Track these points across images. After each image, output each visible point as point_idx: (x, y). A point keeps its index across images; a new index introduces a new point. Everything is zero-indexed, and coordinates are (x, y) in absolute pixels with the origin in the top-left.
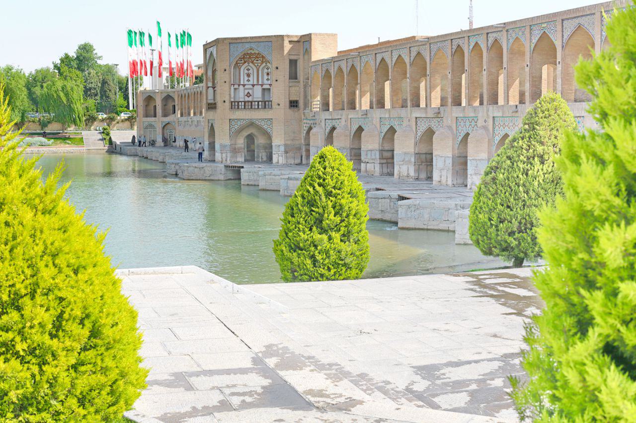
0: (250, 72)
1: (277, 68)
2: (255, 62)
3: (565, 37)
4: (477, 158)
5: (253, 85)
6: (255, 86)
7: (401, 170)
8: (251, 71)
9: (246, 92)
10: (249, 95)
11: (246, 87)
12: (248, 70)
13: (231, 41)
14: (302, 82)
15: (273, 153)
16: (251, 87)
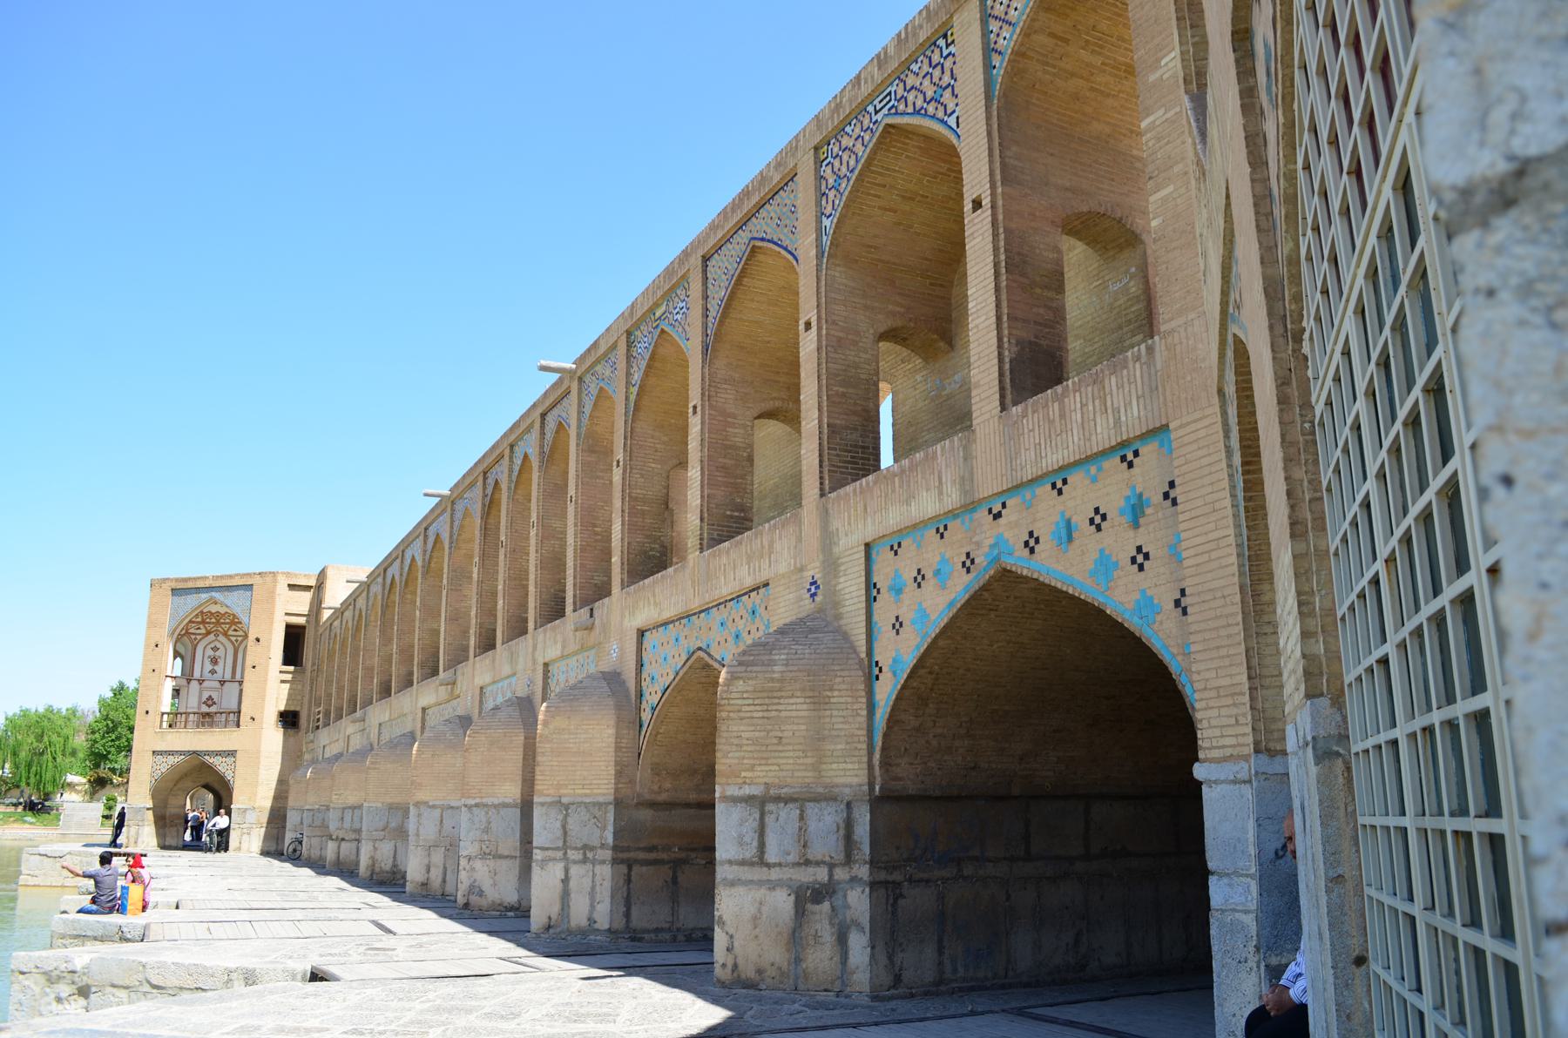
0: (217, 653)
1: (258, 640)
2: (231, 633)
3: (712, 313)
4: (489, 801)
5: (222, 683)
6: (227, 684)
7: (378, 856)
8: (220, 653)
9: (205, 695)
10: (210, 702)
11: (206, 684)
12: (215, 649)
13: (174, 585)
14: (308, 673)
16: (217, 685)
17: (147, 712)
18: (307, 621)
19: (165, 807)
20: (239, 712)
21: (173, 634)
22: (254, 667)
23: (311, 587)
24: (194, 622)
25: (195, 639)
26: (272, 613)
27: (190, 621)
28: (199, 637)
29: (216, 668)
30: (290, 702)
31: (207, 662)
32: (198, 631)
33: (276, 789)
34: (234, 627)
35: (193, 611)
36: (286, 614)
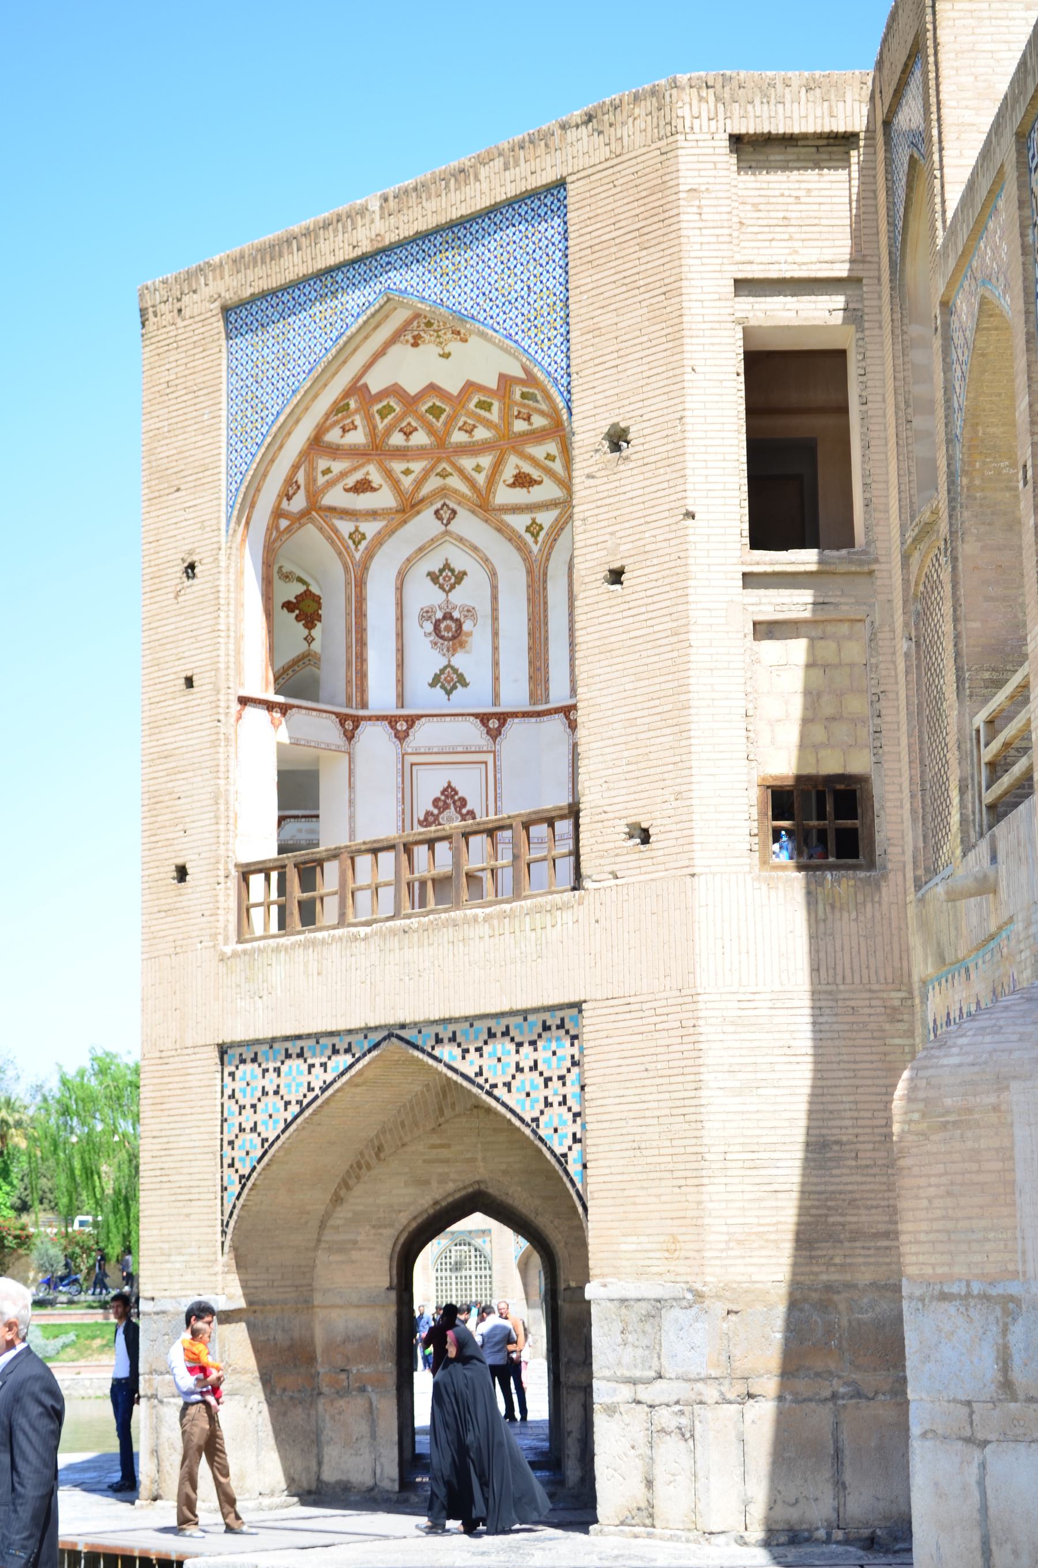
0: (460, 597)
6: (514, 728)
11: (423, 735)
15: (602, 1391)
16: (473, 733)
17: (182, 873)
18: (853, 315)
19: (306, 1304)
20: (574, 812)
21: (249, 503)
22: (616, 576)
23: (848, 139)
24: (335, 451)
25: (357, 537)
26: (672, 290)
27: (317, 444)
28: (370, 528)
29: (460, 661)
30: (819, 733)
31: (419, 638)
32: (364, 501)
33: (805, 1193)
34: (512, 465)
35: (320, 383)
36: (744, 286)
